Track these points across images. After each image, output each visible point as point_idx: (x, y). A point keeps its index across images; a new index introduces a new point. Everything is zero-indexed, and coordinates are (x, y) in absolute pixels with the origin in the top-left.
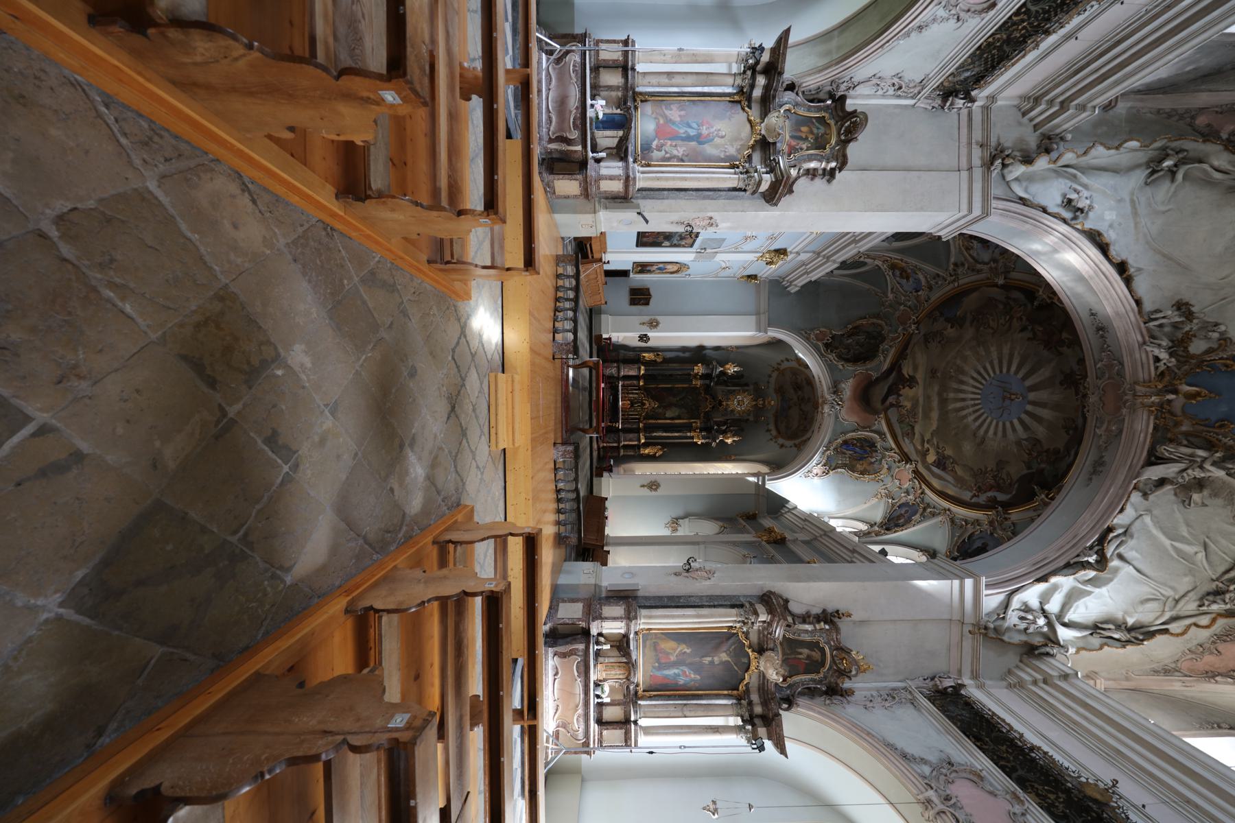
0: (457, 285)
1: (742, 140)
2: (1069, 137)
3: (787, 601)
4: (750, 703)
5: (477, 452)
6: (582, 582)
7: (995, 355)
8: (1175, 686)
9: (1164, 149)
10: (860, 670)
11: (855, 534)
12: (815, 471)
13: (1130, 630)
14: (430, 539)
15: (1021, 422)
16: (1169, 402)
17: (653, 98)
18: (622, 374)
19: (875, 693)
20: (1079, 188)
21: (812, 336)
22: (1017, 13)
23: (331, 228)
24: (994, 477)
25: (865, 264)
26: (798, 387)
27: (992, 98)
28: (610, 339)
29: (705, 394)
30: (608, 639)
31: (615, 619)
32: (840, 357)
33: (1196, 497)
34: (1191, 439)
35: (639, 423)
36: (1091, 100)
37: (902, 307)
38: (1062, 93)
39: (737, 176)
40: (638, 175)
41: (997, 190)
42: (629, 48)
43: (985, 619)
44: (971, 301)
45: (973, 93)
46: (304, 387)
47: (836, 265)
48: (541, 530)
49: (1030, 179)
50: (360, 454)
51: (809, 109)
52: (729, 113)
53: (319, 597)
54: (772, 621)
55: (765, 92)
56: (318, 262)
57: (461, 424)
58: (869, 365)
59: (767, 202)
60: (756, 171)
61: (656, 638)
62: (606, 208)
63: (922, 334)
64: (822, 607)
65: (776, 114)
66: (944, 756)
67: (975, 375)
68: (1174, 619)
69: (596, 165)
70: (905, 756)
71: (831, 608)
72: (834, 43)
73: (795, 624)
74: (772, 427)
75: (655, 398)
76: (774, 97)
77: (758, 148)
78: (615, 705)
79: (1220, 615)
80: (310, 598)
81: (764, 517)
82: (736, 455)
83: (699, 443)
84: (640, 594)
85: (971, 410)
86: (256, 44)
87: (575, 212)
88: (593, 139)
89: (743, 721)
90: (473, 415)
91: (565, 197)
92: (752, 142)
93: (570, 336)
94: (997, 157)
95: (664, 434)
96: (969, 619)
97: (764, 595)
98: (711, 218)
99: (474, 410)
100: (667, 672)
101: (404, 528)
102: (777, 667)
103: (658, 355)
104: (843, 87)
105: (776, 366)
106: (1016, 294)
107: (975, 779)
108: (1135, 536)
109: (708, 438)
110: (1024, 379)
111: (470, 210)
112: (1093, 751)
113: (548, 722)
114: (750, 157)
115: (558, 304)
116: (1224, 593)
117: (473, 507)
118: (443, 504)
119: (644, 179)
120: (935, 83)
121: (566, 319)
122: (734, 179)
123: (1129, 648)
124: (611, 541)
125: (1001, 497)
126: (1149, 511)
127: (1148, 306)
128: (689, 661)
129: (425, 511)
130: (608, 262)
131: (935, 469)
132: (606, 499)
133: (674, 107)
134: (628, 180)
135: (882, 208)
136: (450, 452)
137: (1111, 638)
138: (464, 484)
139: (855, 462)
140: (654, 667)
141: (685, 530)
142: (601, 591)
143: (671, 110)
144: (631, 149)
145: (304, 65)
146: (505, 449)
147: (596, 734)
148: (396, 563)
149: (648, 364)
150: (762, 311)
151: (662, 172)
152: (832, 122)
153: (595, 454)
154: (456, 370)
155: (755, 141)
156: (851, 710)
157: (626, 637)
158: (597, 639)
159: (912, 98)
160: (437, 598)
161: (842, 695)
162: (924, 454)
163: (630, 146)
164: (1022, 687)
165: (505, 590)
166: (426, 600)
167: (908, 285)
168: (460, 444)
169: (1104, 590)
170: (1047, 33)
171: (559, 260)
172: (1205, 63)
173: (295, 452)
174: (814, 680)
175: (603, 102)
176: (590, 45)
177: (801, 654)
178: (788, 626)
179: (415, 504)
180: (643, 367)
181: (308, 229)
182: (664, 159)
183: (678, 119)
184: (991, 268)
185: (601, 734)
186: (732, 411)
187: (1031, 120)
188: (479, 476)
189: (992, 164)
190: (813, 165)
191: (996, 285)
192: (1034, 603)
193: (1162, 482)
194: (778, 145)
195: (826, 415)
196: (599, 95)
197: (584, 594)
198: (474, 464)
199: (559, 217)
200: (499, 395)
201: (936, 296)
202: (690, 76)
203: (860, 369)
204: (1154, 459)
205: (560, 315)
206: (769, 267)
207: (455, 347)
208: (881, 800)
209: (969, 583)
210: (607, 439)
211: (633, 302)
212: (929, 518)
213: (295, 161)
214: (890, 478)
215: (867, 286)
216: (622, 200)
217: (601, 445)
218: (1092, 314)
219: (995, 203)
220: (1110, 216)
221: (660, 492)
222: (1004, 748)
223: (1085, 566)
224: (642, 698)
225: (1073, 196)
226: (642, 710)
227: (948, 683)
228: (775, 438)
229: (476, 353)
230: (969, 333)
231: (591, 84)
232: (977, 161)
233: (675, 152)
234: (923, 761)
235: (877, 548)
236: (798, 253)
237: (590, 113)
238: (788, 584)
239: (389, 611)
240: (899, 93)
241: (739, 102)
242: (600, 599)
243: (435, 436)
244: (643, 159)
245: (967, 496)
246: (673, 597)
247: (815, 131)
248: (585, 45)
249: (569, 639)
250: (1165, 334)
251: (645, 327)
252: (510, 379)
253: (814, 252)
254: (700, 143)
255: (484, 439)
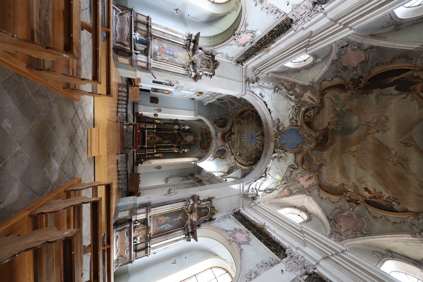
0: (75, 96)
1: (187, 60)
2: (261, 79)
3: (199, 197)
4: (188, 230)
5: (82, 158)
6: (129, 203)
7: (250, 128)
8: (277, 200)
9: (276, 86)
10: (217, 212)
11: (220, 176)
12: (210, 159)
13: (270, 190)
14: (63, 190)
15: (255, 144)
16: (277, 140)
17: (158, 38)
18: (147, 127)
19: (221, 218)
20: (263, 91)
21: (210, 119)
22: (249, 49)
23: (20, 76)
24: (250, 158)
25: (223, 100)
26: (206, 134)
27: (247, 66)
28: (142, 114)
29: (178, 135)
30: (139, 221)
31: (142, 213)
32: (217, 126)
33: (280, 160)
34: (280, 148)
35: (154, 145)
36: (264, 72)
37: (232, 113)
38: (259, 69)
39: (185, 71)
40: (152, 63)
41: (248, 89)
42: (149, 21)
43: (245, 193)
44: (246, 114)
45: (243, 64)
46: (8, 135)
47: (216, 100)
48: (112, 182)
49: (254, 87)
50: (31, 160)
51: (205, 56)
52: (183, 51)
53: (15, 213)
54: (194, 203)
55: (194, 48)
56: (14, 88)
57: (75, 147)
58: (225, 128)
59: (194, 80)
60: (190, 71)
61: (157, 217)
62: (140, 70)
63: (236, 120)
64: (208, 197)
65: (196, 55)
66: (235, 228)
67: (247, 132)
68: (277, 186)
69: (136, 55)
70: (226, 231)
71: (210, 197)
72: (212, 40)
73: (201, 203)
74: (199, 146)
75: (160, 137)
76: (196, 50)
77: (191, 63)
78: (142, 243)
79: (284, 184)
80: (11, 213)
81: (196, 174)
82: (188, 155)
83: (176, 152)
84: (152, 204)
85: (246, 141)
86: (15, 36)
87: (127, 69)
88: (135, 46)
89: (186, 235)
90: (81, 144)
91: (123, 64)
92: (189, 62)
93: (125, 114)
94: (248, 80)
95: (164, 149)
96: (242, 193)
97: (192, 196)
98: (177, 81)
99: (81, 142)
100: (161, 227)
101: (50, 187)
102: (195, 216)
103: (161, 121)
104: (214, 53)
105: (200, 127)
106: (254, 113)
107: (240, 231)
108: (271, 169)
109: (179, 150)
110: (255, 134)
111: (87, 79)
112: (263, 218)
113: (114, 256)
114: (189, 66)
115: (119, 102)
116: (284, 179)
117: (81, 178)
118: (67, 178)
119: (154, 65)
120: (235, 59)
121: (123, 108)
122: (184, 72)
123: (270, 194)
124: (141, 189)
125: (251, 163)
126: (273, 163)
127: (273, 119)
128: (169, 221)
129: (60, 180)
130: (141, 86)
131: (239, 157)
132: (140, 174)
133: (165, 44)
134: (148, 64)
135: (223, 88)
136: (70, 158)
137: (267, 192)
138: (76, 170)
139: (221, 156)
140: (156, 227)
141: (170, 182)
142: (136, 205)
143: (164, 44)
144: (149, 53)
145: (34, 44)
146: (94, 157)
147: (134, 255)
148: (49, 199)
149: (157, 124)
150: (196, 110)
151: (161, 64)
152: (211, 62)
153: (135, 157)
154: (73, 127)
155: (190, 61)
156: (215, 223)
157: (146, 219)
158: (135, 222)
159: (231, 61)
160: (72, 206)
161: (213, 220)
162: (236, 153)
163: (149, 52)
164: (252, 207)
165: (100, 200)
166: (67, 207)
167: (233, 108)
168: (75, 155)
169: (266, 182)
170: (255, 55)
171: (119, 85)
172: (282, 70)
173: (4, 159)
174: (206, 218)
175: (139, 35)
176: (134, 15)
177: (202, 211)
178: (199, 204)
179: (55, 178)
180: (155, 125)
181: (11, 76)
182: (161, 59)
183: (167, 48)
184: (250, 106)
185: (136, 255)
186: (187, 141)
187: (254, 73)
188: (83, 167)
189: (247, 82)
190: (206, 72)
191: (250, 110)
192: (254, 188)
193: (275, 157)
194: (197, 64)
195: (214, 142)
196: (137, 31)
197: (130, 208)
198: (81, 162)
199: (120, 70)
200: (93, 136)
201: (239, 111)
202: (170, 36)
203: (222, 129)
204: (274, 152)
205: (120, 106)
206: (198, 97)
207: (73, 118)
208: (219, 243)
209: (242, 184)
210: (140, 152)
211: (152, 102)
212: (237, 170)
213: (10, 55)
214: (229, 160)
215: (224, 106)
216: (147, 69)
217: (138, 154)
218: (265, 120)
219: (247, 92)
220: (268, 99)
221: (161, 170)
222: (246, 222)
223: (263, 177)
224: (153, 238)
225: (261, 93)
226: (152, 242)
227: (237, 210)
228: (200, 149)
229: (82, 120)
230: (246, 122)
231: (134, 26)
232: (244, 81)
233: (165, 58)
234: (230, 231)
235: (224, 179)
236: (206, 94)
237: (133, 37)
238: (200, 192)
239: (50, 213)
240: (227, 58)
241: (186, 48)
242: (136, 208)
243: (64, 152)
244: (154, 57)
245: (245, 163)
246: (164, 202)
247: (207, 63)
248: (132, 14)
249: (123, 225)
250: (276, 126)
251: (156, 111)
252: (98, 130)
253: (210, 95)
254: (174, 57)
255: (85, 153)
